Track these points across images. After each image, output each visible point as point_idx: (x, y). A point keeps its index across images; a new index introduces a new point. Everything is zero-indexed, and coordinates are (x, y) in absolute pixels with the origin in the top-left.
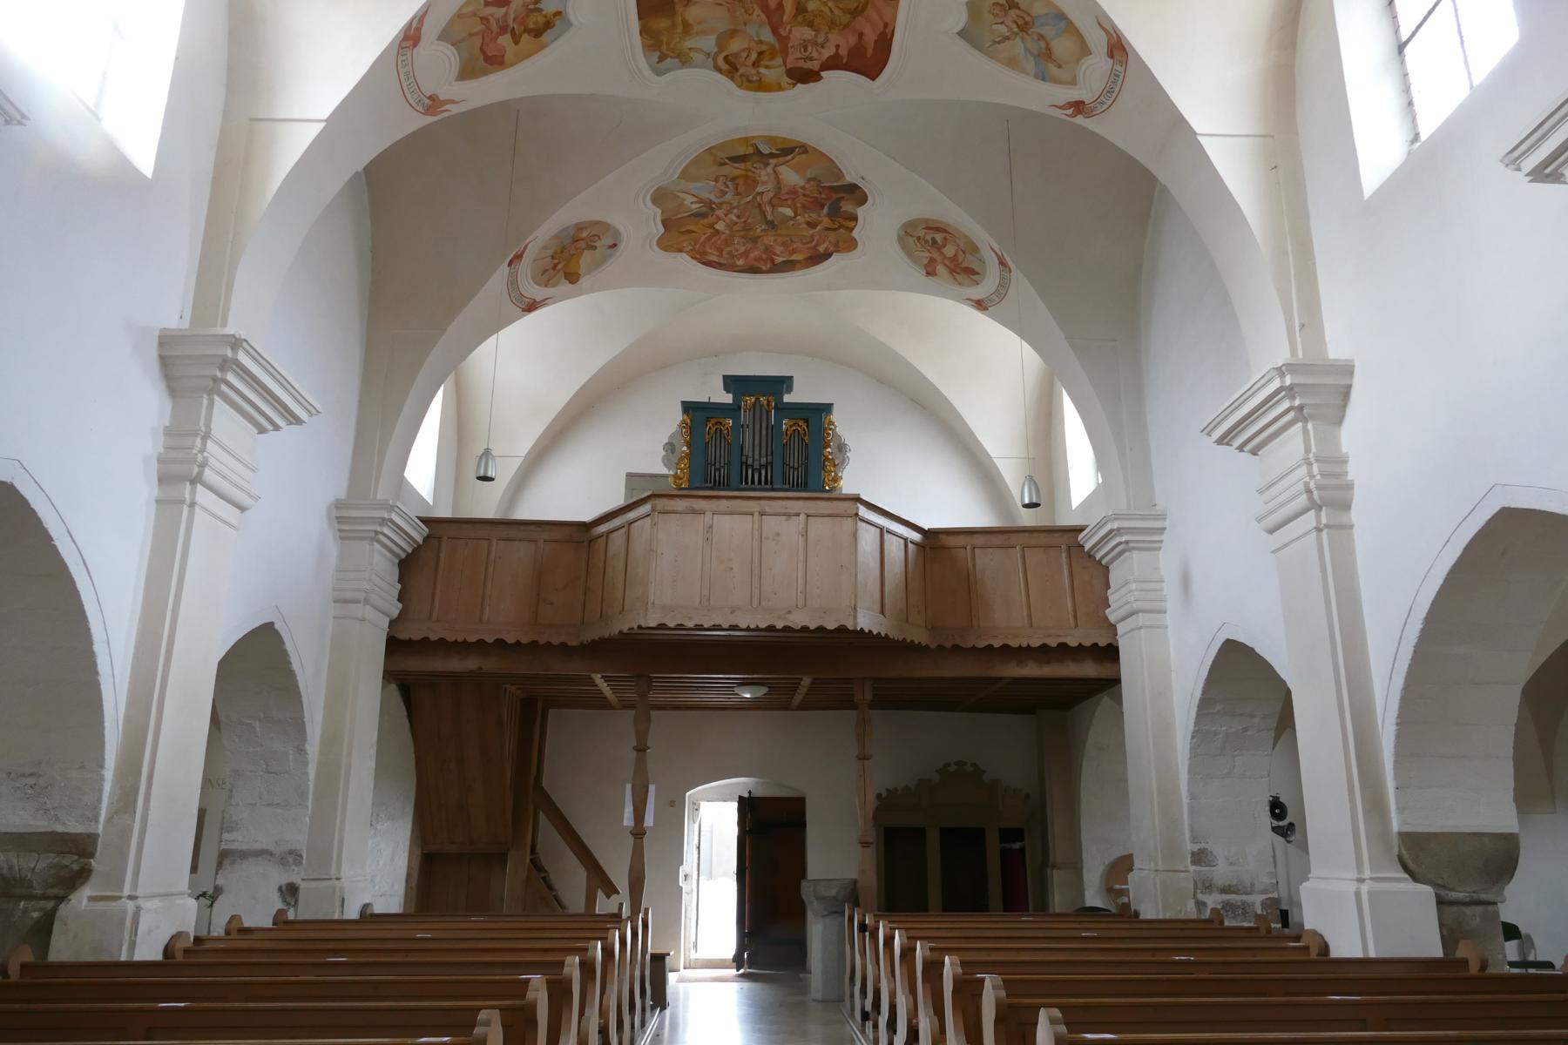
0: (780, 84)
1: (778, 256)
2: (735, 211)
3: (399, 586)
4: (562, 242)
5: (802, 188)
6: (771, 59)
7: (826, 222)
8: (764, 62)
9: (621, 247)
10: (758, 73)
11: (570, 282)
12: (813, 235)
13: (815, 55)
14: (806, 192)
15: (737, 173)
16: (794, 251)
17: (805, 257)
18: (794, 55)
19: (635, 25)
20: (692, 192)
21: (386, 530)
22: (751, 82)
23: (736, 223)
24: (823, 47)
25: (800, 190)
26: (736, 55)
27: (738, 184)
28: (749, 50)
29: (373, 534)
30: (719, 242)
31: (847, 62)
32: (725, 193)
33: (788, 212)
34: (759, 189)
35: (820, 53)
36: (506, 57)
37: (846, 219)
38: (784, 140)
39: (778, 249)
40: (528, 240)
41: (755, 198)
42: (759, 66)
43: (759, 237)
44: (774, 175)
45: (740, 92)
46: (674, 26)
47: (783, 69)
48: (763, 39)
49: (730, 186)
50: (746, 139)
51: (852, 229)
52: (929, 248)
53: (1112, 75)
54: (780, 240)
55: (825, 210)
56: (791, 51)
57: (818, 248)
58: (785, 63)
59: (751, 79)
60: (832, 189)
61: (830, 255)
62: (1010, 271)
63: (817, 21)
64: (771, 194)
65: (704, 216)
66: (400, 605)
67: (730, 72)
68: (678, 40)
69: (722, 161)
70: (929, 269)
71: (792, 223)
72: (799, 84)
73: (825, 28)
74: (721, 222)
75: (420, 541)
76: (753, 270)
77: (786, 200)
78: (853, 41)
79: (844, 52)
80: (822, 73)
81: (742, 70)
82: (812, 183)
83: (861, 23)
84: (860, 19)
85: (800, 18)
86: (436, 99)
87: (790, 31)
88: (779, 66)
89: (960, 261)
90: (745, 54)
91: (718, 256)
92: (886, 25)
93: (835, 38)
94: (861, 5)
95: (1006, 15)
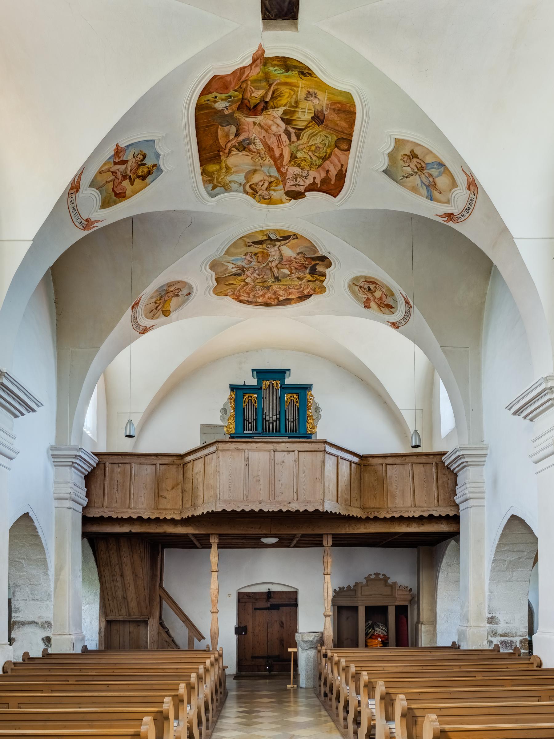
0: (281, 200)
1: (281, 296)
2: (257, 272)
3: (86, 489)
4: (160, 294)
5: (295, 258)
6: (276, 186)
7: (309, 277)
9: (193, 295)
11: (165, 316)
12: (301, 284)
13: (302, 183)
14: (297, 261)
16: (290, 294)
17: (297, 296)
20: (232, 262)
21: (77, 461)
22: (265, 199)
23: (258, 279)
24: (306, 178)
26: (257, 184)
27: (258, 257)
29: (71, 464)
32: (251, 262)
33: (287, 272)
34: (270, 259)
37: (319, 276)
38: (285, 231)
39: (281, 293)
40: (141, 295)
41: (268, 264)
42: (269, 190)
43: (271, 286)
44: (278, 252)
45: (259, 205)
46: (221, 168)
47: (283, 192)
48: (272, 174)
49: (254, 258)
50: (262, 232)
51: (323, 281)
53: (469, 199)
55: (308, 271)
56: (288, 181)
58: (284, 188)
60: (313, 259)
61: (311, 295)
62: (411, 307)
63: (303, 163)
64: (277, 262)
65: (239, 275)
66: (87, 500)
67: (253, 194)
69: (249, 244)
72: (293, 200)
73: (307, 168)
75: (95, 465)
76: (267, 305)
77: (286, 265)
78: (323, 175)
79: (318, 181)
80: (306, 194)
81: (260, 193)
82: (300, 255)
83: (328, 165)
84: (327, 162)
85: (293, 162)
86: (90, 221)
87: (287, 169)
90: (261, 184)
92: (342, 166)
93: (313, 173)
95: (411, 162)
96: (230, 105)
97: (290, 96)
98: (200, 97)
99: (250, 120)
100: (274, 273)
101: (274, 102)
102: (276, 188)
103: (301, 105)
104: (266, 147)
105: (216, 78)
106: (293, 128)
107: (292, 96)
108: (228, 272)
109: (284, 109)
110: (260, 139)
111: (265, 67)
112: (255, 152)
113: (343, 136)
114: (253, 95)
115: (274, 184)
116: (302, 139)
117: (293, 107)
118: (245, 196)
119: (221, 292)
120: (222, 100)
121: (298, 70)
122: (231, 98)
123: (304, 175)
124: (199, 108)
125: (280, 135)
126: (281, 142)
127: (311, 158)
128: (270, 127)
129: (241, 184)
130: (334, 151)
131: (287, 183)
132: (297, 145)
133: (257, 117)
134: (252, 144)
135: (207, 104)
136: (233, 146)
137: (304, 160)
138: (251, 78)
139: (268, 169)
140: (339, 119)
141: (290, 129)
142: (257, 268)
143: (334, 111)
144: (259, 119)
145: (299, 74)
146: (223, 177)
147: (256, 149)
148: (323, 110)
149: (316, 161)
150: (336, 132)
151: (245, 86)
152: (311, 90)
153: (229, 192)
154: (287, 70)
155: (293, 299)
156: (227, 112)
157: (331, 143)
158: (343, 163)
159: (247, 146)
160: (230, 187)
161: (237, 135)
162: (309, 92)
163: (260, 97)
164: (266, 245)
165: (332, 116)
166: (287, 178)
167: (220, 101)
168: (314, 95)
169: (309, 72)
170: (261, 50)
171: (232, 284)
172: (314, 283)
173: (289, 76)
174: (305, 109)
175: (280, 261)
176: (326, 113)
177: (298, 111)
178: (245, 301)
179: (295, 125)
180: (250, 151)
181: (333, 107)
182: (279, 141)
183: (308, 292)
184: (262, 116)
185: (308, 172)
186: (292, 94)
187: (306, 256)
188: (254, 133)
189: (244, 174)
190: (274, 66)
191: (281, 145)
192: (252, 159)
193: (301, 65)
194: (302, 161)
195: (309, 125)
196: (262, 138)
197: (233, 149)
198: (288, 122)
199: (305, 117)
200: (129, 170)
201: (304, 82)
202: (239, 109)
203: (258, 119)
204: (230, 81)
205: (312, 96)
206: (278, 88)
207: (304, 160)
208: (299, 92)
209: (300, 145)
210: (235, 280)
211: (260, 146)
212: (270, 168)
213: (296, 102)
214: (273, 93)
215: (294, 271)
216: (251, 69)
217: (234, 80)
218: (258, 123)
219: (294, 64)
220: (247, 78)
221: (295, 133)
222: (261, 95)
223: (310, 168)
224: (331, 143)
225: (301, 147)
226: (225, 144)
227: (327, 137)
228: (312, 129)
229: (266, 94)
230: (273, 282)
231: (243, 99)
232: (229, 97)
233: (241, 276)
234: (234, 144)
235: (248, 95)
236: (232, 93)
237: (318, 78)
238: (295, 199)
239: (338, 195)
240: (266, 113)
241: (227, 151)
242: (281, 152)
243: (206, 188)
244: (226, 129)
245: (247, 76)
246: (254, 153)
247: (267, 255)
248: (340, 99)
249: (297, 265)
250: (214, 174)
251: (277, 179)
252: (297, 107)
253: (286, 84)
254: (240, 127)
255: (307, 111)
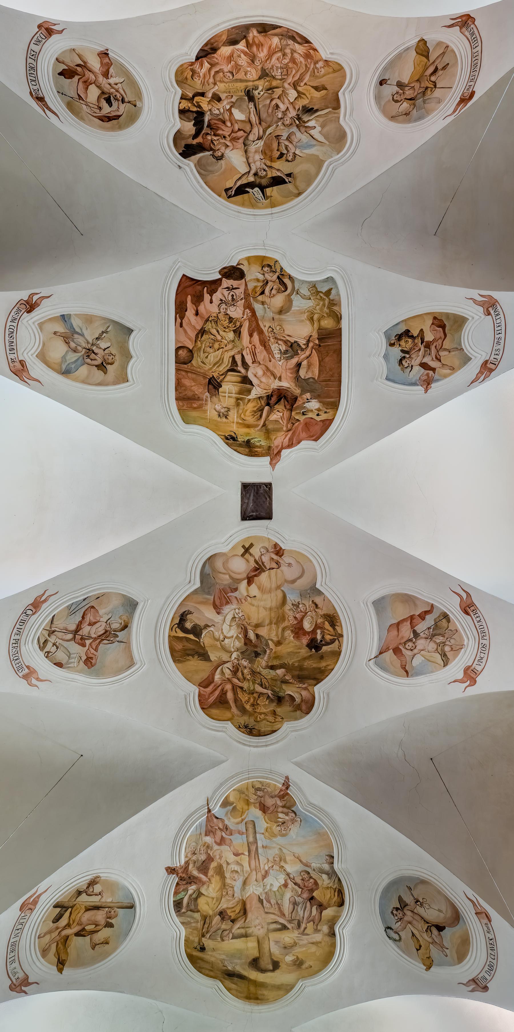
0: (249, 264)
2: (280, 115)
5: (227, 146)
6: (256, 287)
8: (260, 284)
10: (264, 274)
12: (215, 84)
13: (226, 293)
14: (223, 141)
15: (278, 164)
16: (230, 58)
17: (219, 52)
18: (239, 293)
19: (344, 325)
22: (269, 266)
23: (278, 98)
24: (221, 300)
25: (229, 144)
26: (279, 291)
27: (278, 150)
28: (271, 296)
30: (294, 72)
31: (204, 288)
32: (288, 139)
33: (238, 115)
34: (261, 143)
35: (223, 294)
36: (431, 322)
38: (243, 205)
39: (243, 61)
41: (264, 132)
42: (264, 281)
43: (260, 78)
44: (251, 160)
45: (276, 256)
46: (319, 321)
47: (248, 277)
48: (261, 306)
49: (284, 148)
50: (273, 205)
52: (112, 90)
54: (241, 75)
55: (206, 119)
56: (242, 296)
57: (209, 66)
58: (246, 285)
59: (269, 269)
60: (201, 148)
61: (197, 58)
63: (226, 323)
64: (251, 137)
67: (283, 275)
68: (318, 307)
69: (290, 179)
70: (106, 60)
71: (234, 99)
72: (235, 265)
73: (221, 316)
74: (292, 101)
77: (239, 130)
78: (201, 308)
79: (207, 297)
80: (220, 277)
81: (275, 277)
82: (220, 154)
83: (197, 323)
84: (199, 328)
85: (238, 324)
87: (243, 314)
88: (251, 280)
89: (81, 84)
90: (274, 292)
91: (295, 52)
93: (214, 309)
94: (199, 339)
96: (304, 403)
97: (245, 411)
98: (333, 419)
99: (285, 384)
100: (254, 110)
101: (260, 405)
102: (256, 284)
103: (233, 401)
104: (268, 346)
105: (316, 438)
106: (239, 372)
107: (243, 412)
108: (321, 120)
109: (250, 396)
110: (274, 358)
111: (269, 445)
112: (280, 340)
113: (186, 366)
114: (281, 414)
115: (259, 290)
116: (230, 357)
117: (241, 399)
118: (293, 274)
119: (334, 71)
120: (312, 411)
121: (238, 442)
122: (303, 412)
123: (224, 306)
124: (335, 406)
125: (253, 363)
126: (252, 353)
127: (218, 331)
128: (264, 374)
129: (298, 294)
130: (192, 343)
131: (243, 292)
132: (234, 350)
133: (278, 387)
134: (283, 351)
135: (327, 409)
136: (303, 350)
137: (225, 328)
138: (283, 433)
139: (266, 315)
140: (193, 388)
141: (243, 371)
142: (280, 124)
143: (198, 397)
144: (276, 384)
145: (237, 438)
146: (318, 307)
147: (279, 344)
148: (211, 397)
149: (212, 327)
150: (194, 370)
151: (289, 426)
152: (224, 420)
153: (312, 281)
154: (248, 442)
155: (224, 44)
156: (308, 395)
157: (198, 354)
158: (181, 329)
159: (289, 348)
160: (310, 289)
161: (299, 365)
162: (226, 417)
163: (275, 411)
164: (267, 175)
165: (200, 390)
166: (244, 300)
167: (314, 410)
168: (221, 414)
169: (227, 441)
170: (273, 464)
171: (317, 88)
172: (196, 91)
173: (247, 436)
174: (229, 397)
175: (248, 139)
176: (207, 394)
177: (236, 394)
178: (299, 39)
179: (238, 376)
180: (286, 342)
181: (201, 402)
182: (254, 354)
183: (202, 65)
184: (272, 387)
185: (219, 310)
186: (242, 415)
187: (211, 152)
188: (280, 367)
189: (293, 309)
190: (260, 447)
191: (252, 349)
192: (284, 330)
193: (235, 448)
194: (227, 326)
195: (223, 376)
196: (272, 359)
197: (304, 347)
198: (245, 380)
199: (228, 387)
200: (421, 352)
201: (231, 429)
202: (296, 399)
203: (276, 385)
204: (302, 432)
205: (223, 413)
206: (257, 421)
207: (225, 328)
208: (235, 417)
209: (231, 349)
210: (311, 97)
211: (275, 348)
212: (264, 316)
213: (238, 405)
214: (261, 416)
215: (227, 116)
216: (282, 443)
217: (299, 433)
218: (277, 379)
219: (242, 449)
220: (287, 433)
221: (237, 366)
222: (273, 413)
223: (218, 316)
224: (198, 354)
225: (230, 346)
226: (313, 354)
227: (203, 363)
228: (220, 372)
229: (268, 416)
230: (256, 88)
231: (291, 410)
232: (305, 413)
233: (303, 107)
234: (303, 353)
235: (286, 414)
236: (302, 418)
237: (219, 435)
238: (233, 267)
239: (181, 279)
240: (269, 391)
241: (311, 345)
242: (252, 339)
243: (339, 295)
244: (310, 375)
245: (286, 436)
246: (282, 338)
247: (266, 154)
248: (194, 414)
249: (223, 130)
250: (327, 314)
251: (255, 298)
252: (238, 399)
253: (248, 426)
254: (296, 376)
255: (227, 395)
